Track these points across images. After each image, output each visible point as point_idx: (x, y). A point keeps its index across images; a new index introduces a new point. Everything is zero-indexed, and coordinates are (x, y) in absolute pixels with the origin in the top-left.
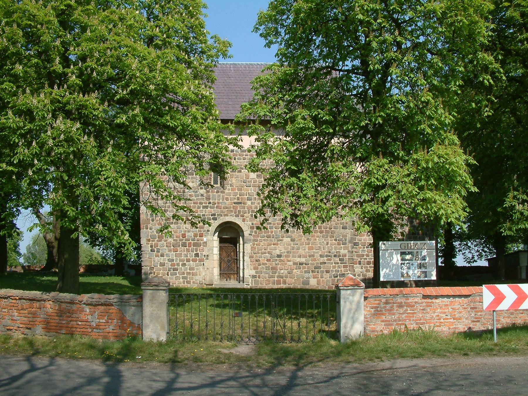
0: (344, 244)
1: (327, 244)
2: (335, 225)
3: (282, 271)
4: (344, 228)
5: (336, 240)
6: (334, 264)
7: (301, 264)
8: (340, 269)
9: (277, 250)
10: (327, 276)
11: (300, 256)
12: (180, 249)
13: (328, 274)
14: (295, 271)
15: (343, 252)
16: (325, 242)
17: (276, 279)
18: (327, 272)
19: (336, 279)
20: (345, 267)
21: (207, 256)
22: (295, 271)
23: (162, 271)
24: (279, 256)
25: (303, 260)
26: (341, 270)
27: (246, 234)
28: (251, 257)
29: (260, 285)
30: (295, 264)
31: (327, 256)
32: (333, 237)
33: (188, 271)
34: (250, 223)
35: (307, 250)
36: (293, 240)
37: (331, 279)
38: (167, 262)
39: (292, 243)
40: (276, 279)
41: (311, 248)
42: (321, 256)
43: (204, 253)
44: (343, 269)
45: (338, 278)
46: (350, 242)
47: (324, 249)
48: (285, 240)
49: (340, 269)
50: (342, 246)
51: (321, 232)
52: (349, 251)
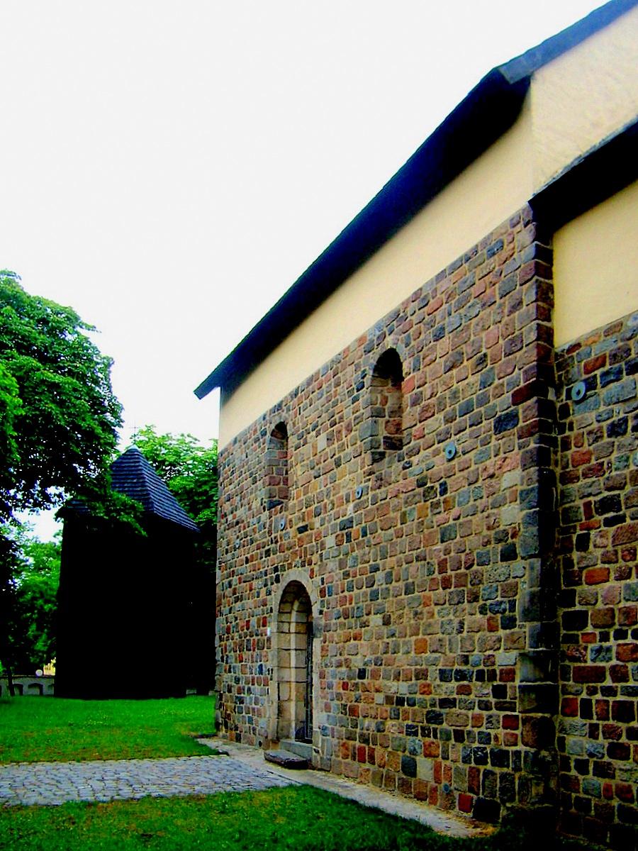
0: (509, 623)
1: (461, 624)
2: (481, 550)
3: (367, 722)
4: (509, 555)
5: (483, 610)
6: (477, 710)
7: (400, 701)
8: (493, 732)
9: (359, 656)
10: (456, 750)
11: (397, 678)
12: (246, 654)
13: (460, 746)
14: (389, 723)
15: (505, 658)
16: (456, 621)
17: (357, 744)
18: (459, 736)
19: (482, 768)
20: (510, 723)
21: (272, 670)
22: (389, 723)
23: (229, 704)
24: (362, 674)
25: (402, 688)
26: (496, 738)
27: (315, 609)
28: (322, 676)
29: (333, 757)
30: (389, 700)
31: (461, 676)
32: (476, 599)
33: (253, 706)
34: (318, 579)
35: (413, 654)
36: (386, 622)
37: (467, 767)
38: (233, 684)
39: (385, 630)
40: (357, 744)
41: (421, 648)
42: (444, 676)
43: (269, 665)
44: (501, 732)
45: (489, 767)
46: (528, 615)
47: (451, 650)
48: (371, 624)
49: (493, 732)
50: (502, 633)
51: (446, 584)
52: (523, 656)
